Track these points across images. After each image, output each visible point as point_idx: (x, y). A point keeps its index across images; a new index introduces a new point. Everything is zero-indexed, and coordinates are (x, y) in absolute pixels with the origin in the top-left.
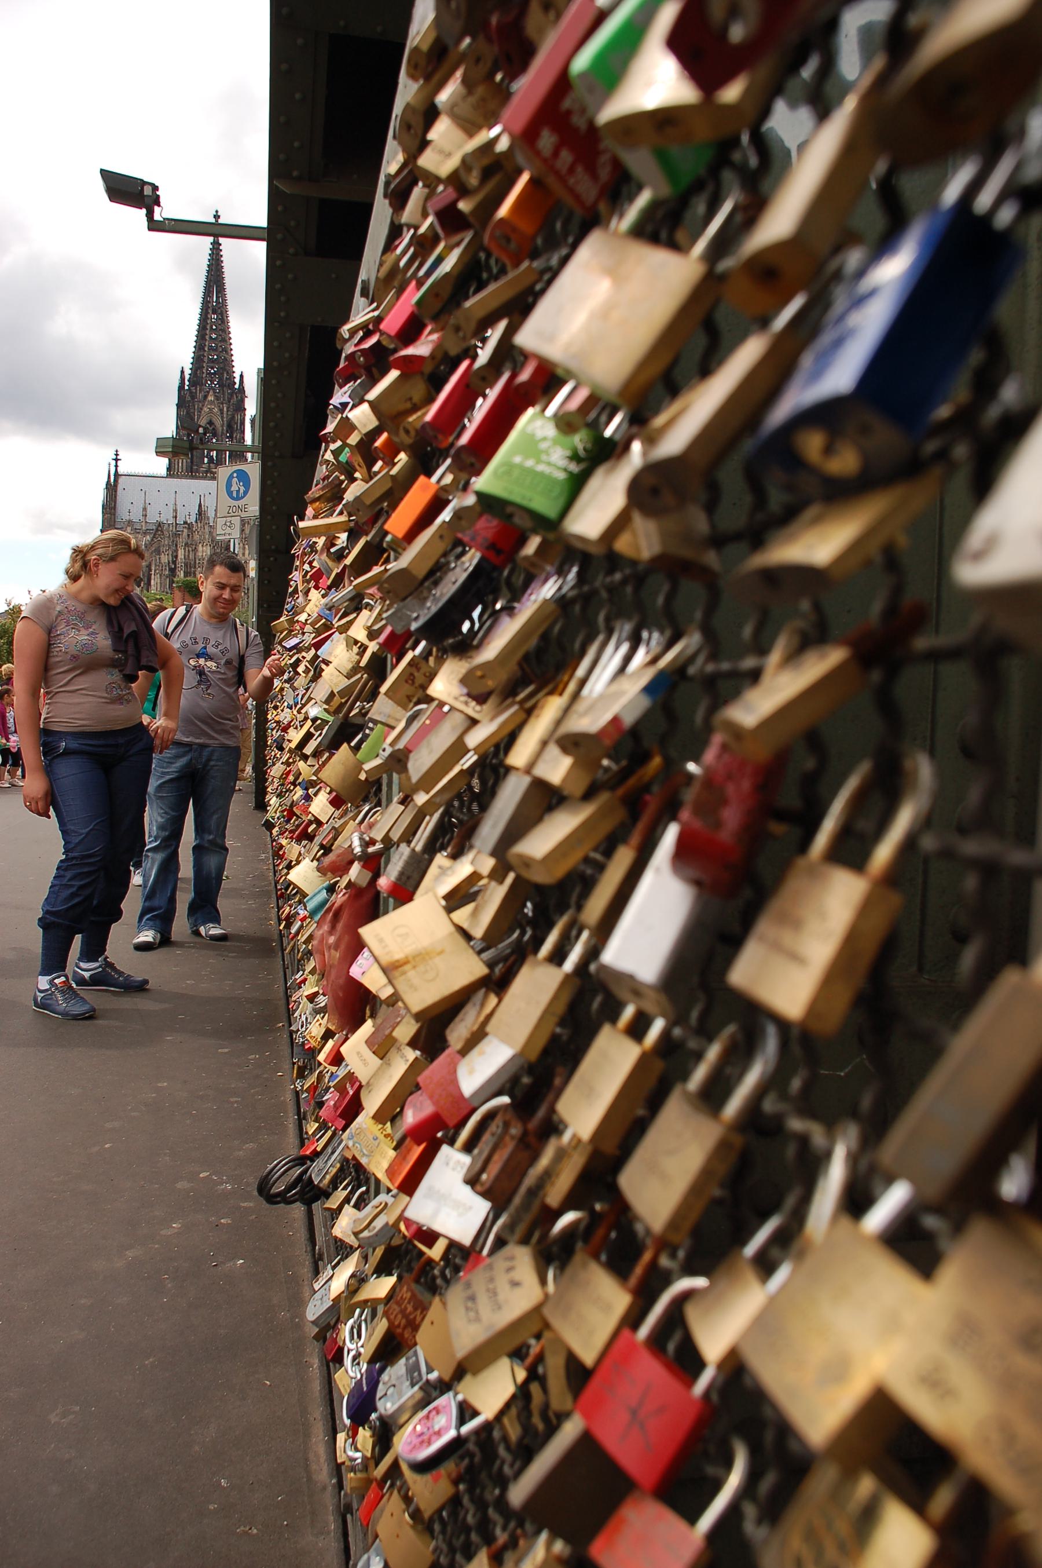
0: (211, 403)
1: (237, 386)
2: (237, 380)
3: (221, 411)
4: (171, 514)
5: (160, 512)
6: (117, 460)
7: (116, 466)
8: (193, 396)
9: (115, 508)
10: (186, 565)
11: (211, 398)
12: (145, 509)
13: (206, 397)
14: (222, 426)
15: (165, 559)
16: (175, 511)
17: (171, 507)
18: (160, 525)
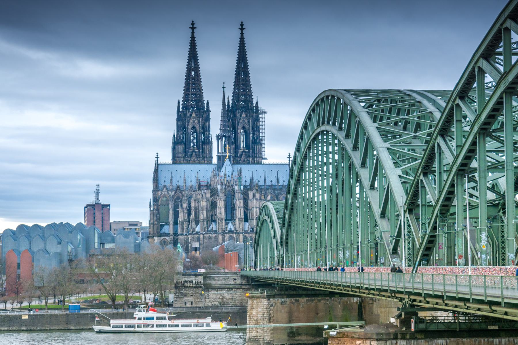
0: (194, 118)
1: (206, 108)
2: (205, 105)
3: (199, 121)
4: (183, 181)
5: (178, 181)
6: (157, 158)
7: (157, 160)
8: (185, 115)
9: (158, 180)
10: (195, 208)
11: (194, 115)
12: (171, 180)
13: (191, 115)
14: (200, 129)
15: (185, 205)
16: (185, 180)
17: (183, 179)
18: (178, 187)
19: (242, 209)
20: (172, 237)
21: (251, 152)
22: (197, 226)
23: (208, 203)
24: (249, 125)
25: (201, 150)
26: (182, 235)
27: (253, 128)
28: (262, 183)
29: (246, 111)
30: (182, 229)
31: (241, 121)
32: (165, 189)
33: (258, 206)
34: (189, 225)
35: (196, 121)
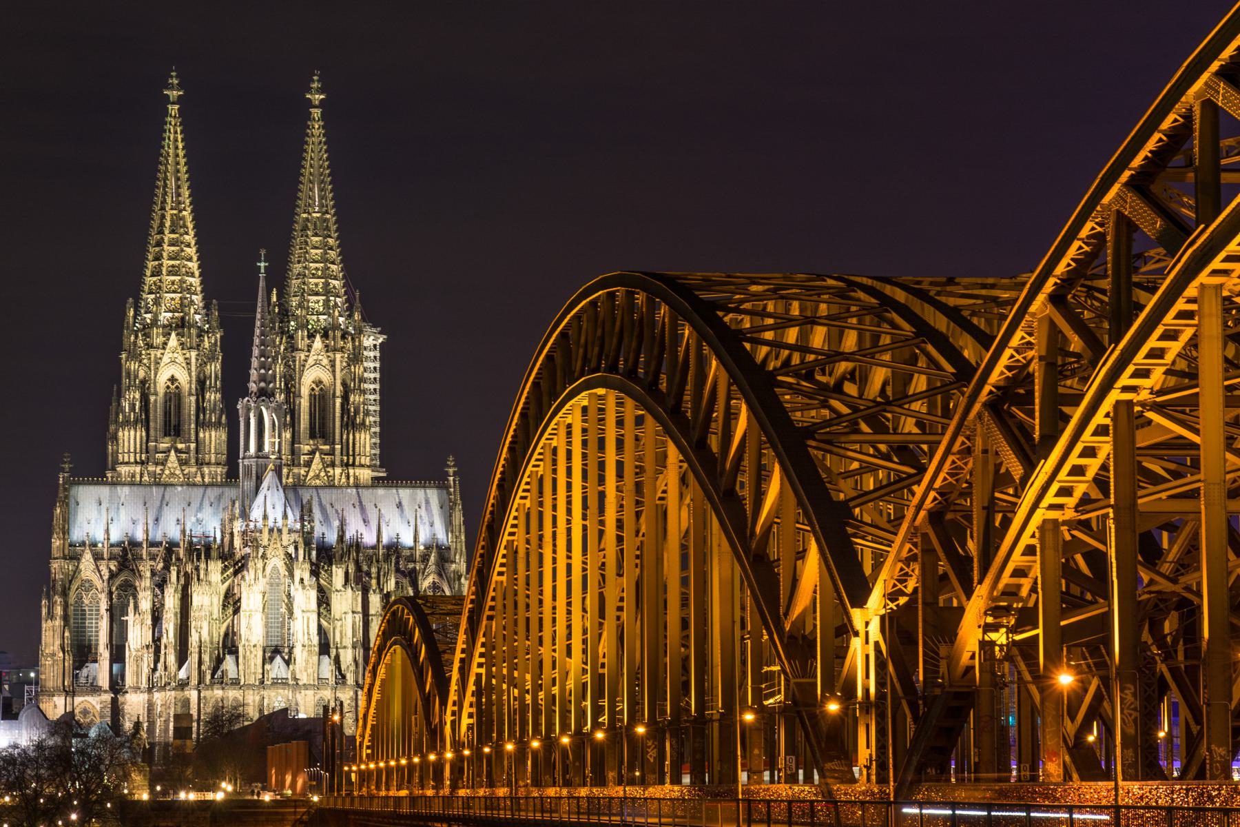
14: (190, 383)
15: (145, 604)
19: (314, 617)
20: (107, 697)
21: (338, 452)
22: (180, 667)
23: (215, 600)
24: (334, 372)
25: (193, 446)
26: (137, 689)
27: (344, 384)
28: (369, 539)
29: (325, 336)
30: (138, 674)
31: (311, 361)
32: (88, 557)
33: (360, 609)
34: (157, 661)
35: (180, 359)
